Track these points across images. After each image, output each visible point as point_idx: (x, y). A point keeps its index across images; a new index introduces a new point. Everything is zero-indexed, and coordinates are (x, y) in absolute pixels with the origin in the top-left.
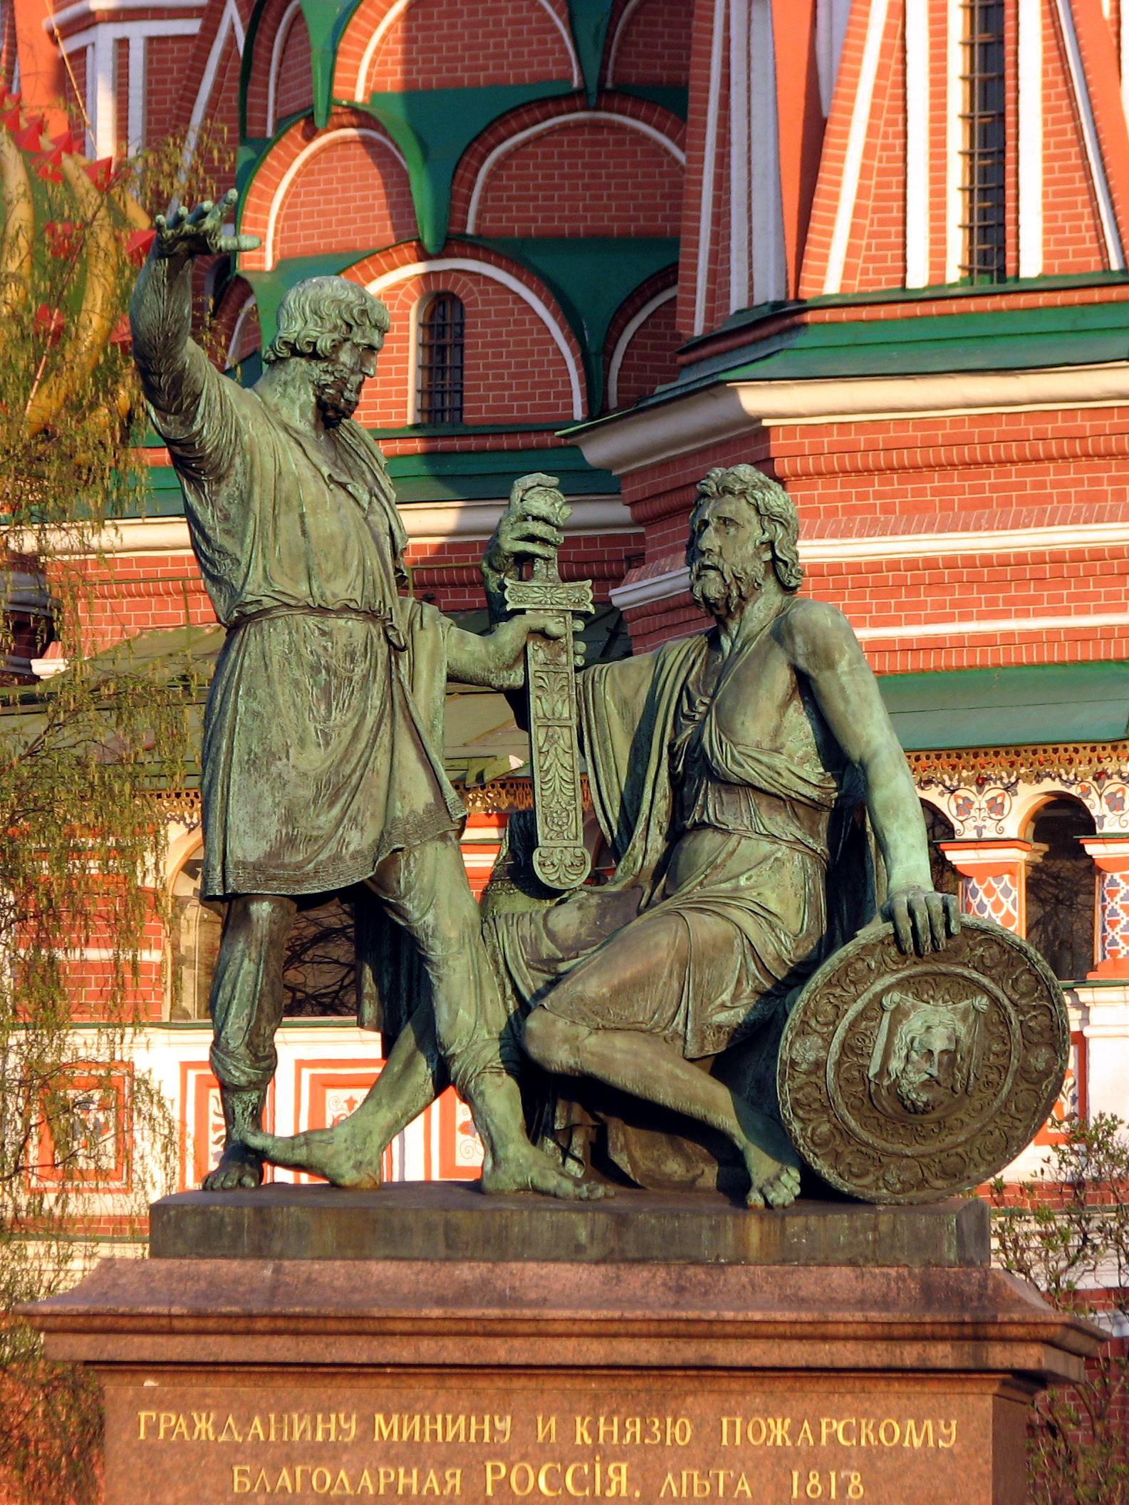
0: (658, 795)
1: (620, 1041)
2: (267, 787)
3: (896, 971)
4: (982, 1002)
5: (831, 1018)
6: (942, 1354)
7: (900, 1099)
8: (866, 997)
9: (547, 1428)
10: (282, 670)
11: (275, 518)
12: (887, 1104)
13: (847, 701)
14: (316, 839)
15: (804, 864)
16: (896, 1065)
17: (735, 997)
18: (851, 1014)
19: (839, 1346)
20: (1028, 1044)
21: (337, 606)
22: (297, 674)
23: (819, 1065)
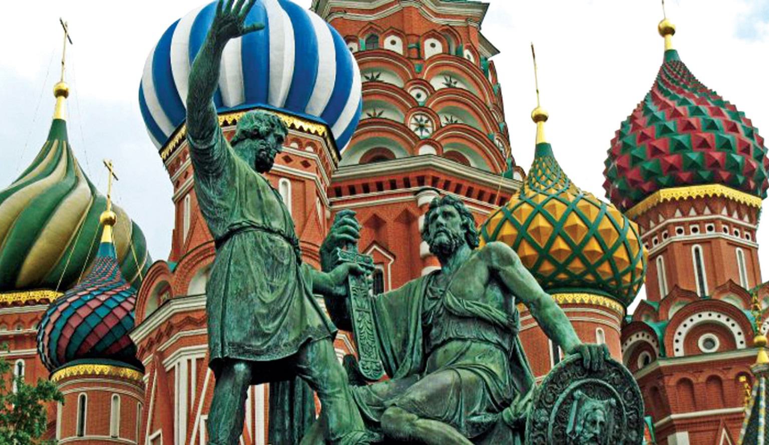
0: (417, 337)
1: (433, 422)
2: (246, 304)
3: (579, 380)
4: (613, 401)
5: (552, 400)
8: (567, 391)
10: (252, 255)
11: (246, 191)
13: (523, 277)
14: (269, 334)
15: (502, 355)
17: (480, 411)
18: (560, 399)
20: (630, 429)
21: (276, 230)
22: (259, 257)
23: (545, 425)
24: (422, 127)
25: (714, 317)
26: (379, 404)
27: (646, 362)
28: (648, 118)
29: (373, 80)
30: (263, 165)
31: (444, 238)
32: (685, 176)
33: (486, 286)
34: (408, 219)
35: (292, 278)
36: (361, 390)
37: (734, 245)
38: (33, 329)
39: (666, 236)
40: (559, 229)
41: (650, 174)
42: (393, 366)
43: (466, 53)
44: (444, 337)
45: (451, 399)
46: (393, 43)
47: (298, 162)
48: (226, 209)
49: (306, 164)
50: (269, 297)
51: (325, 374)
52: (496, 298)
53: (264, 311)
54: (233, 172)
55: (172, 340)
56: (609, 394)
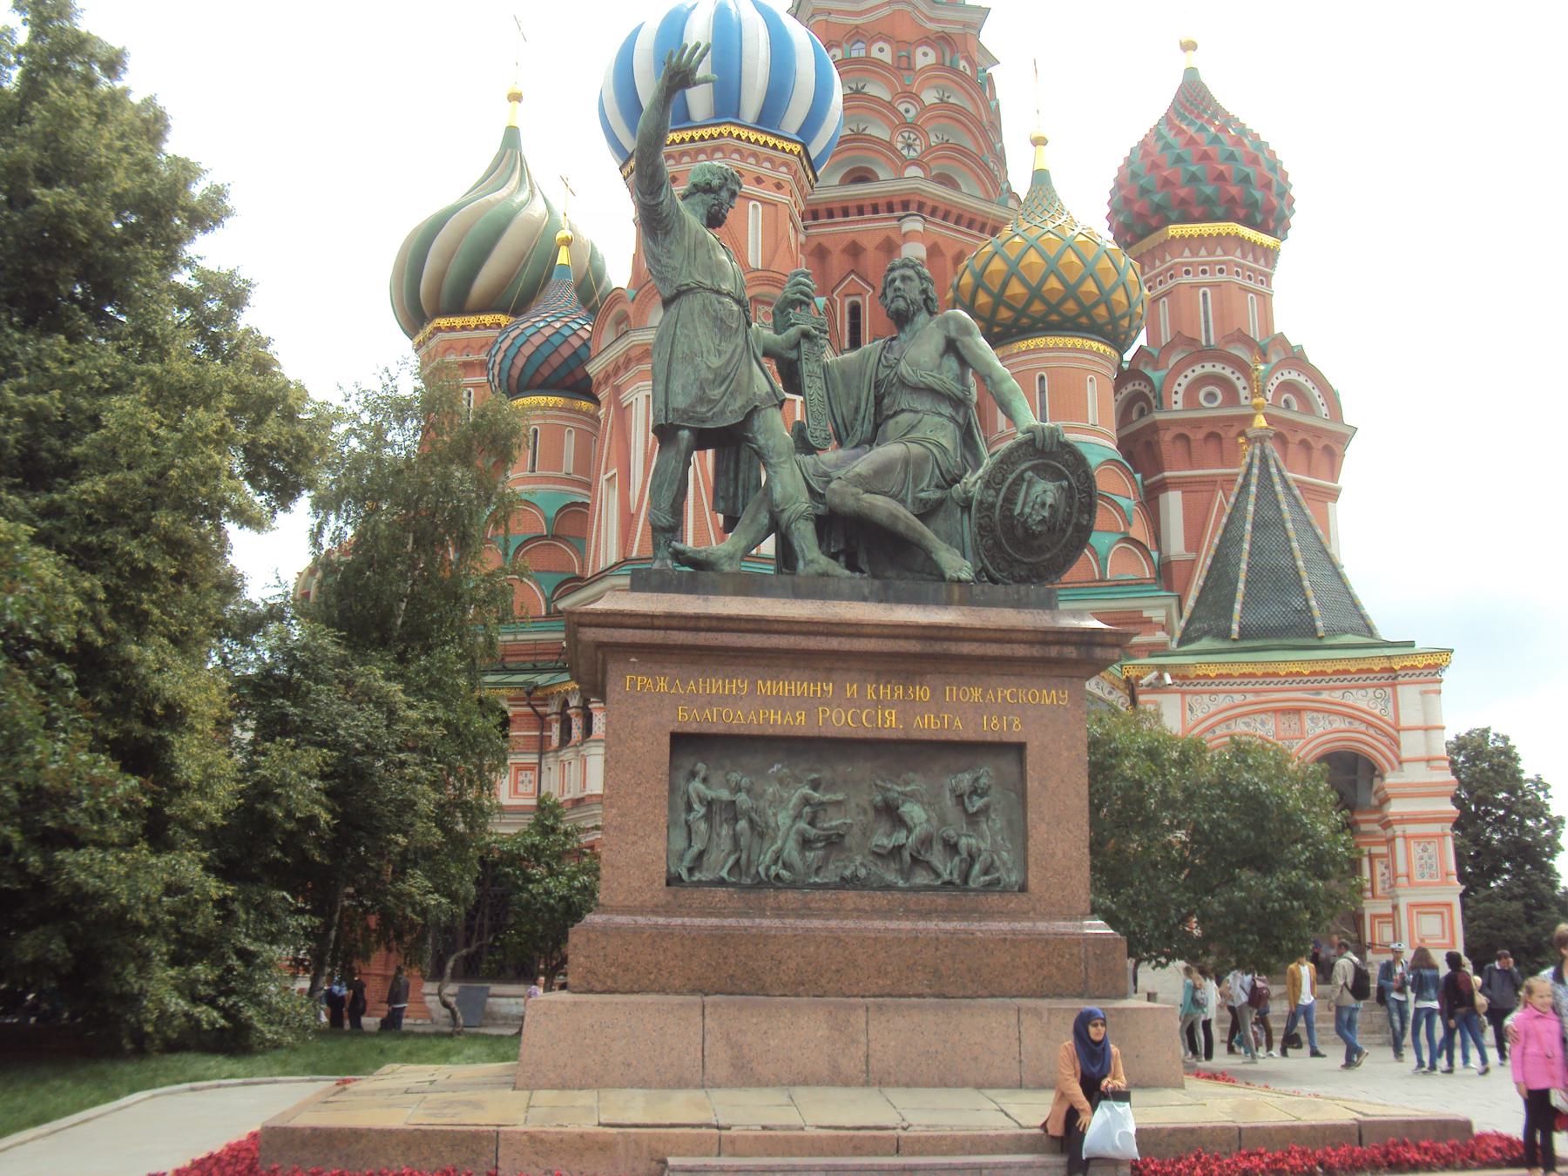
6: (1071, 652)
7: (1026, 529)
9: (852, 690)
12: (1020, 532)
16: (1027, 510)
19: (1015, 646)
20: (1081, 512)
23: (993, 505)
24: (909, 146)
25: (1218, 369)
26: (826, 475)
27: (1142, 413)
28: (1161, 144)
29: (857, 91)
30: (714, 220)
31: (901, 304)
32: (1196, 213)
33: (942, 356)
34: (889, 247)
35: (740, 341)
36: (808, 459)
37: (1246, 290)
38: (483, 356)
39: (1172, 277)
40: (1053, 270)
41: (1159, 208)
42: (844, 434)
43: (962, 64)
44: (896, 408)
45: (898, 475)
46: (881, 50)
47: (769, 183)
48: (674, 269)
49: (779, 186)
50: (715, 362)
51: (771, 443)
52: (951, 369)
53: (711, 377)
54: (682, 228)
55: (630, 374)
56: (1058, 476)
